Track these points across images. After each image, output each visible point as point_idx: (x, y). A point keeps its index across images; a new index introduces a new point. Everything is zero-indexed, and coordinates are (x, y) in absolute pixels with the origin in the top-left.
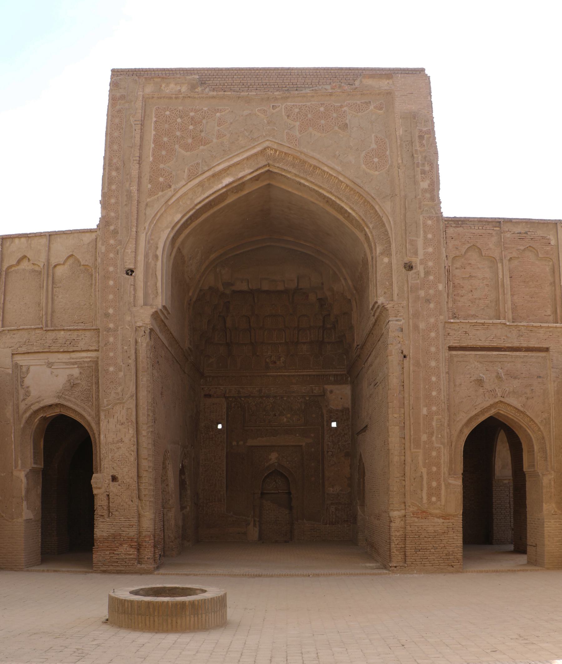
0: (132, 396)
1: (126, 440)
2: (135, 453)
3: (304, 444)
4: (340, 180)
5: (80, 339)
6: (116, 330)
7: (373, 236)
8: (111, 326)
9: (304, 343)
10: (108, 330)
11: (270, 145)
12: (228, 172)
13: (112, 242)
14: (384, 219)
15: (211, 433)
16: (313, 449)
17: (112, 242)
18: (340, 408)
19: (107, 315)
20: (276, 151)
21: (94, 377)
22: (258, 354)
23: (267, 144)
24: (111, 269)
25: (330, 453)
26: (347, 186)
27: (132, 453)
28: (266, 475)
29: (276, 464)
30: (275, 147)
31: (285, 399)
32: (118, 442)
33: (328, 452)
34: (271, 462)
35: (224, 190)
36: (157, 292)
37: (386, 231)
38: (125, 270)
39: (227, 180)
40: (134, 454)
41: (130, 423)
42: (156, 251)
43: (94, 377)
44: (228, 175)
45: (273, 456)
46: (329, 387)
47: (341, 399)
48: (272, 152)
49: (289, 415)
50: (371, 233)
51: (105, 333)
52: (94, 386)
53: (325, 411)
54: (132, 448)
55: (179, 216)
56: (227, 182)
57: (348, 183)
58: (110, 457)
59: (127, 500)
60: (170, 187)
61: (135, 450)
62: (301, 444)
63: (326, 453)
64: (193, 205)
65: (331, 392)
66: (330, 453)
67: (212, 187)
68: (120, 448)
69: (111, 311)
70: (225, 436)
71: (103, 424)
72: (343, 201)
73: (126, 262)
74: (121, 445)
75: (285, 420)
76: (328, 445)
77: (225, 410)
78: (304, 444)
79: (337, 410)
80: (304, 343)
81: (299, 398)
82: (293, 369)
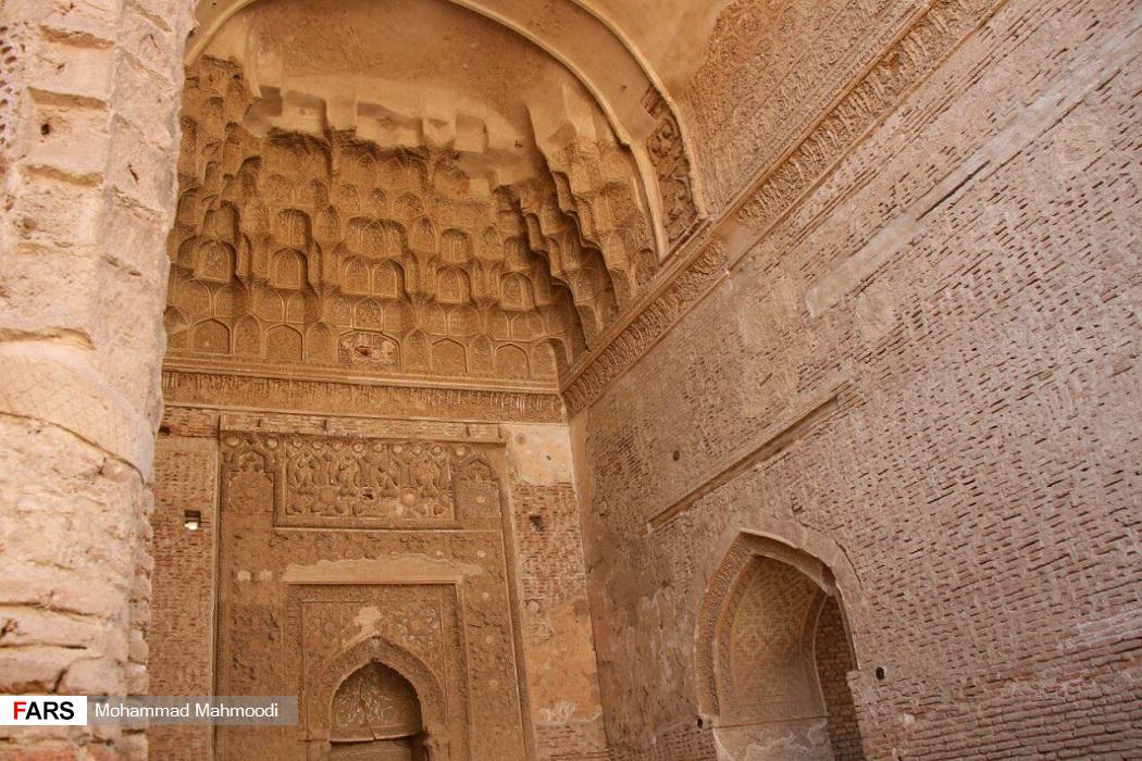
3: (459, 580)
9: (448, 307)
15: (167, 542)
16: (486, 595)
18: (548, 481)
22: (323, 320)
25: (534, 606)
28: (344, 677)
29: (376, 643)
31: (398, 449)
33: (527, 602)
34: (361, 637)
45: (368, 619)
46: (513, 428)
47: (549, 458)
49: (410, 497)
53: (508, 490)
62: (449, 579)
63: (522, 605)
65: (521, 440)
66: (534, 606)
70: (213, 552)
75: (400, 510)
76: (526, 582)
77: (214, 474)
78: (459, 580)
79: (541, 488)
80: (448, 307)
81: (437, 450)
82: (419, 372)
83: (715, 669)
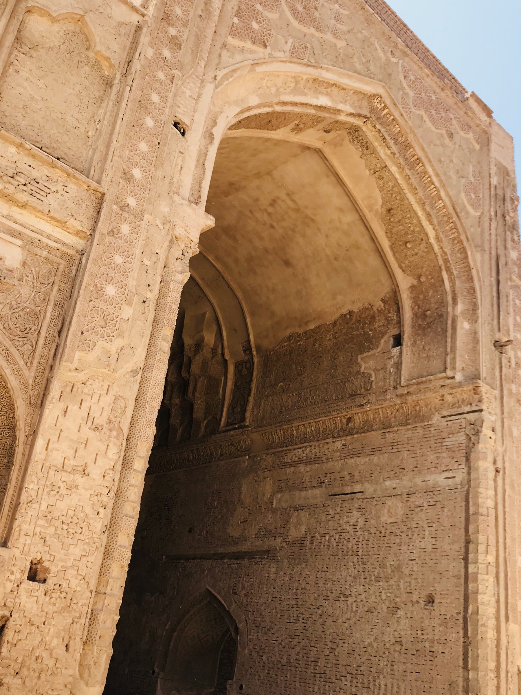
0: (135, 372)
1: (95, 472)
2: (109, 511)
4: (440, 195)
5: (54, 189)
6: (139, 216)
7: (453, 286)
8: (132, 201)
10: (124, 207)
11: (383, 95)
12: (329, 90)
13: (167, 53)
14: (474, 272)
17: (167, 53)
19: (128, 177)
20: (385, 107)
21: (56, 289)
23: (380, 91)
24: (155, 98)
26: (444, 207)
27: (101, 510)
30: (388, 102)
32: (74, 471)
35: (313, 111)
36: (200, 197)
37: (474, 289)
38: (174, 119)
39: (324, 101)
40: (105, 515)
41: (114, 433)
42: (212, 129)
43: (56, 289)
44: (327, 94)
48: (380, 107)
50: (452, 281)
51: (115, 207)
52: (50, 308)
54: (105, 499)
55: (254, 101)
56: (324, 104)
57: (448, 204)
58: (44, 507)
59: (55, 642)
60: (265, 46)
61: (110, 505)
64: (276, 100)
67: (305, 95)
68: (76, 487)
69: (137, 173)
71: (52, 411)
72: (431, 223)
73: (179, 107)
74: (80, 480)
83: (170, 648)
